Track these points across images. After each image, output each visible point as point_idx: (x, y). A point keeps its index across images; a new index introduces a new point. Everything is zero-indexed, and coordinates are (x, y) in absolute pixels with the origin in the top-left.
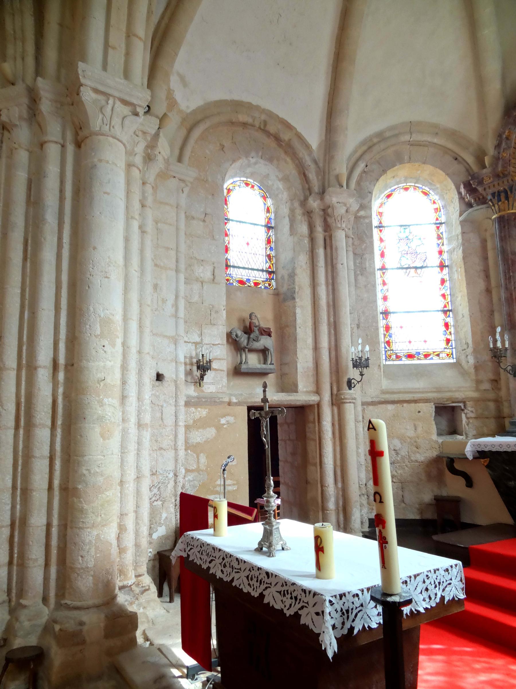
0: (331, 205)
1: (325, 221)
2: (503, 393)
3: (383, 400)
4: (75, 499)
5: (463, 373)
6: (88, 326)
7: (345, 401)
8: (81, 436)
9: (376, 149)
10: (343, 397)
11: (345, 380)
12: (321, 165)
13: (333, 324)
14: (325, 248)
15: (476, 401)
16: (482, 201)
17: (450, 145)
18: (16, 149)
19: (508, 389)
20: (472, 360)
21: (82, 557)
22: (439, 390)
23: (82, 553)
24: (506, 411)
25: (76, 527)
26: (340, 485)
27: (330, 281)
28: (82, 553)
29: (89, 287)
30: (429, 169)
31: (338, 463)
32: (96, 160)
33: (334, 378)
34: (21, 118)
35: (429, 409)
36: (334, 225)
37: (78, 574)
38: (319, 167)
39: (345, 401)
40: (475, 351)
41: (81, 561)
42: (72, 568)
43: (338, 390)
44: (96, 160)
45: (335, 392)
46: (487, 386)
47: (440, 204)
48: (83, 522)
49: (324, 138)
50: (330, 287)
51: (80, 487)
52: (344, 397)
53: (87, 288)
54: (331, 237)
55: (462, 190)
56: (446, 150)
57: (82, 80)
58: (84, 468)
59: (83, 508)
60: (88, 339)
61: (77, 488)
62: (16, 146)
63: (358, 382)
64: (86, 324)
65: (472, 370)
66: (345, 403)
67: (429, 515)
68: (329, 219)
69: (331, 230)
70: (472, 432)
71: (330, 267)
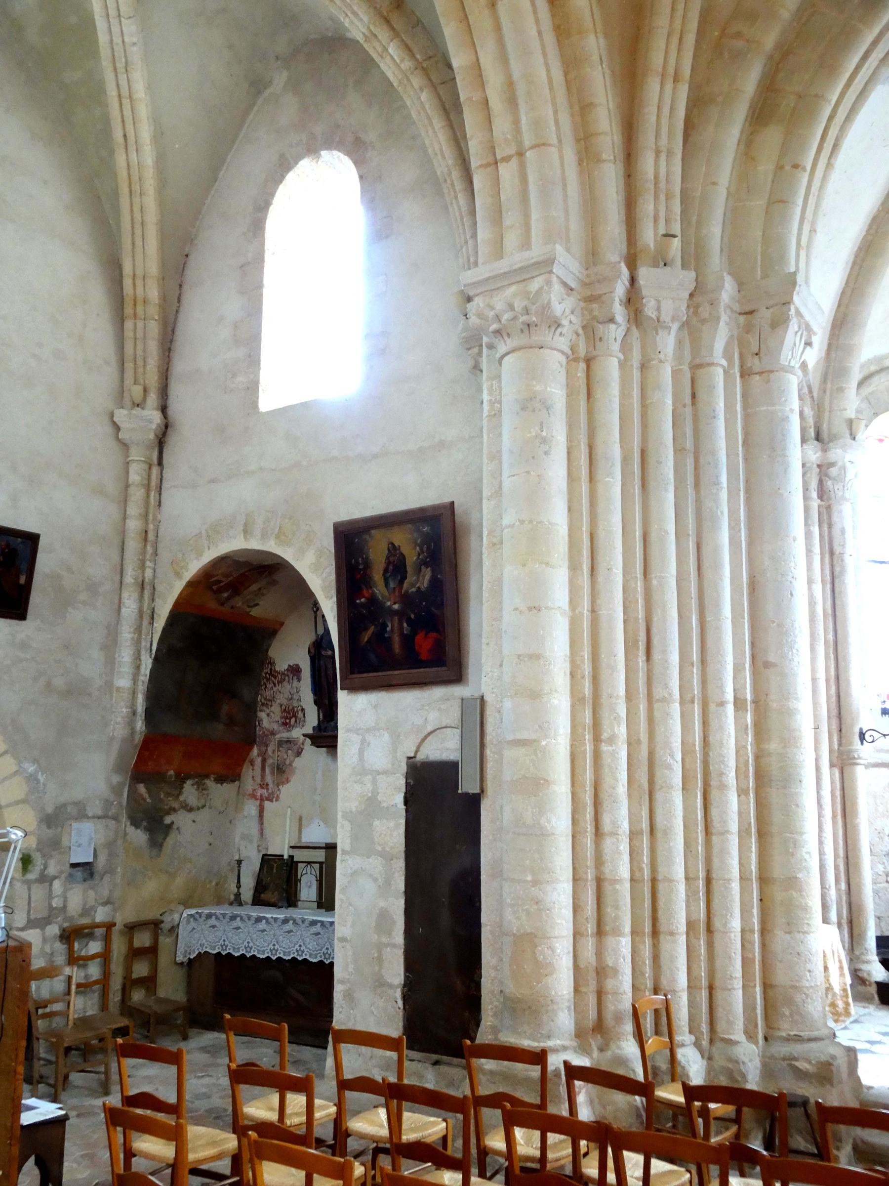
0: (840, 464)
1: (821, 483)
3: (880, 761)
4: (794, 893)
6: (795, 651)
7: (858, 761)
8: (797, 805)
9: (875, 380)
10: (856, 756)
11: (857, 731)
12: (815, 395)
13: (832, 643)
14: (820, 526)
18: (661, 361)
21: (809, 971)
23: (809, 966)
25: (799, 932)
26: (843, 886)
27: (828, 578)
28: (809, 966)
29: (792, 595)
31: (841, 853)
32: (787, 409)
33: (835, 727)
34: (673, 319)
36: (840, 494)
37: (807, 996)
38: (812, 397)
39: (858, 761)
41: (808, 976)
42: (795, 987)
43: (840, 744)
44: (787, 409)
45: (836, 747)
48: (808, 924)
49: (823, 354)
50: (828, 587)
51: (800, 875)
52: (858, 756)
53: (789, 596)
54: (829, 508)
57: (796, 298)
58: (804, 850)
59: (806, 904)
60: (796, 668)
61: (796, 878)
62: (662, 356)
63: (884, 735)
64: (791, 647)
66: (858, 764)
68: (829, 484)
69: (829, 499)
71: (827, 556)
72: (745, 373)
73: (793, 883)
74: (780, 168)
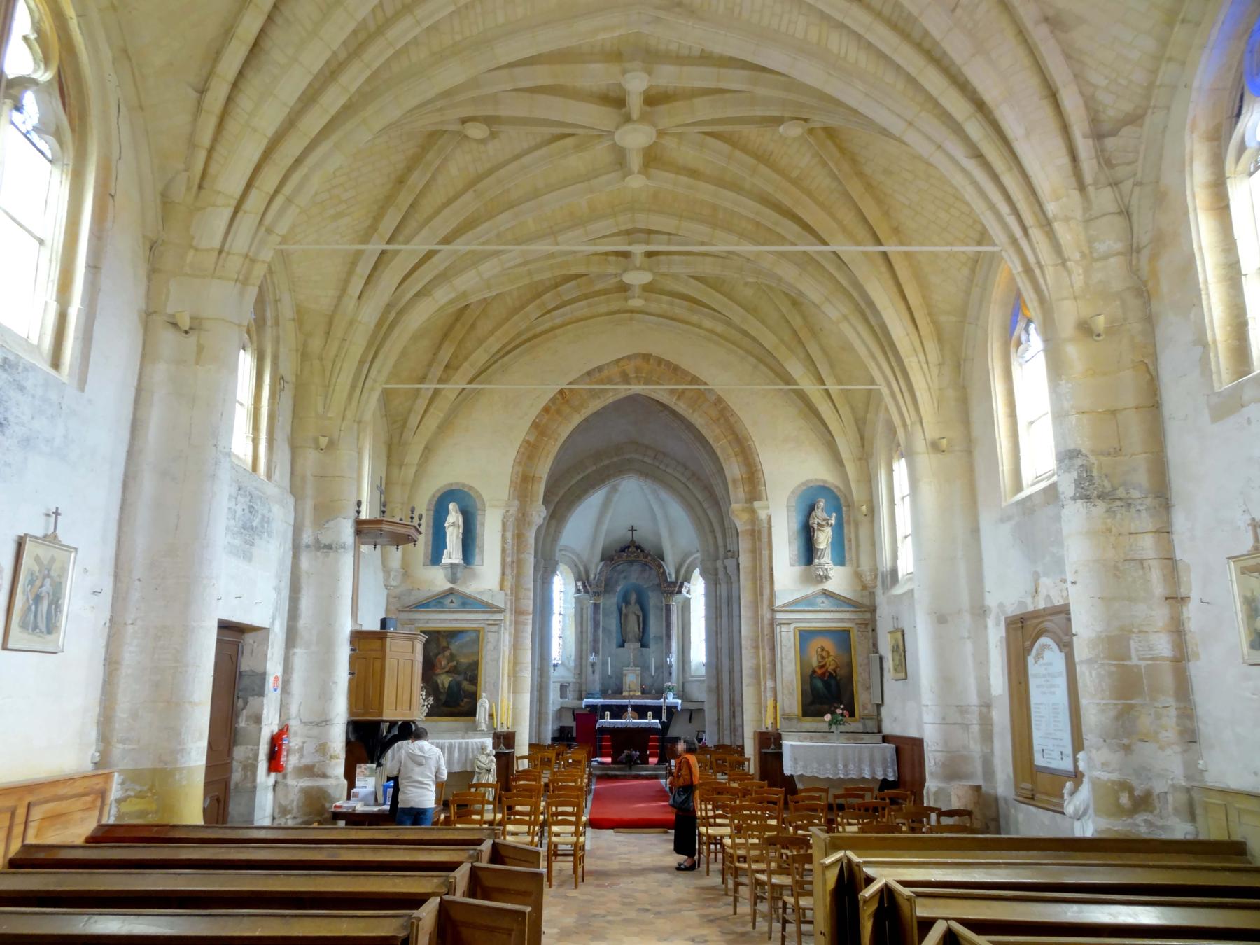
2: (584, 680)
5: (568, 669)
15: (575, 683)
16: (587, 592)
17: (577, 561)
19: (586, 678)
20: (572, 664)
22: (563, 677)
24: (584, 688)
30: (566, 567)
35: (558, 686)
40: (575, 660)
46: (577, 676)
47: (562, 582)
55: (579, 584)
56: (573, 561)
65: (573, 668)
67: (556, 736)
70: (571, 697)
72: (543, 583)
73: (547, 713)
74: (555, 531)
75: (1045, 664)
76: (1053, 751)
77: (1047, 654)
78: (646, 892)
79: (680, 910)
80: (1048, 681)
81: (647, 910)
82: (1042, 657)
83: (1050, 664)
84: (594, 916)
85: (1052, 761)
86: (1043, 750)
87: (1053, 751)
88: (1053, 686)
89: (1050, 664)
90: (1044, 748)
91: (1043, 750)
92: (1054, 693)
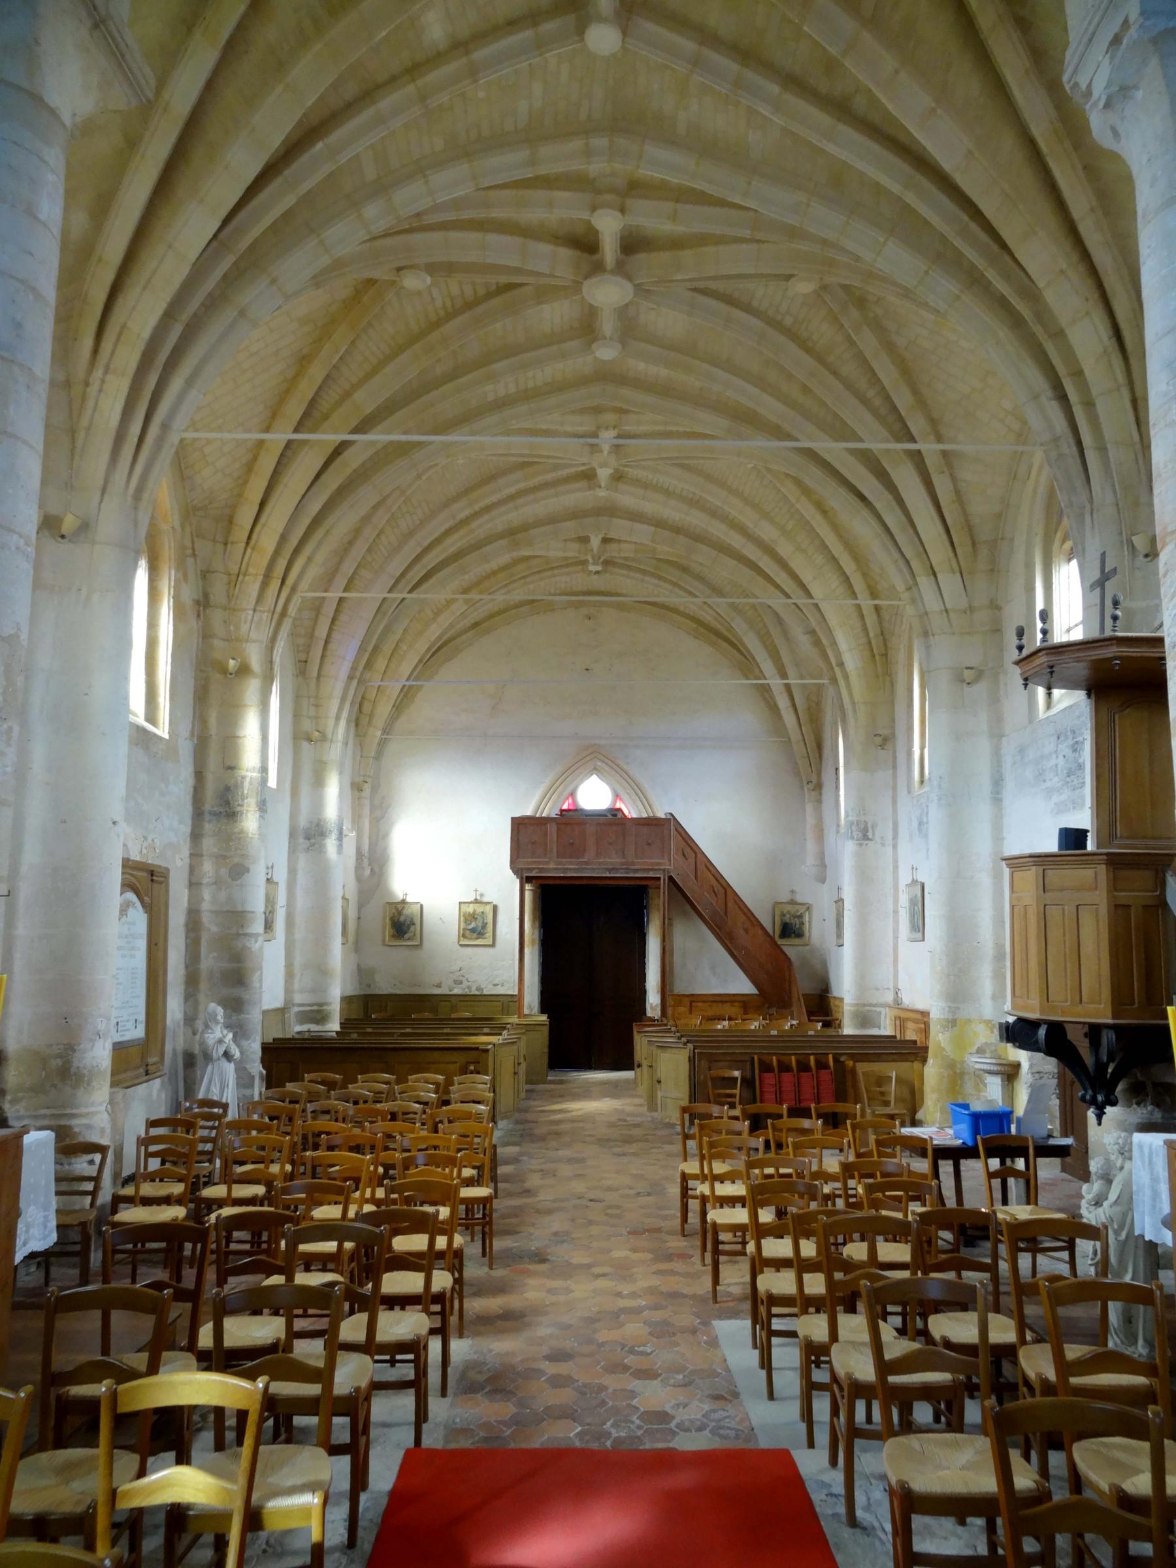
75: (129, 923)
76: (128, 1021)
77: (131, 911)
78: (591, 1222)
79: (554, 1201)
80: (129, 942)
81: (591, 1200)
82: (126, 915)
83: (133, 924)
84: (649, 1194)
85: (127, 1033)
86: (117, 1023)
87: (128, 1021)
88: (133, 948)
89: (133, 924)
90: (119, 1020)
91: (117, 1023)
92: (133, 956)
